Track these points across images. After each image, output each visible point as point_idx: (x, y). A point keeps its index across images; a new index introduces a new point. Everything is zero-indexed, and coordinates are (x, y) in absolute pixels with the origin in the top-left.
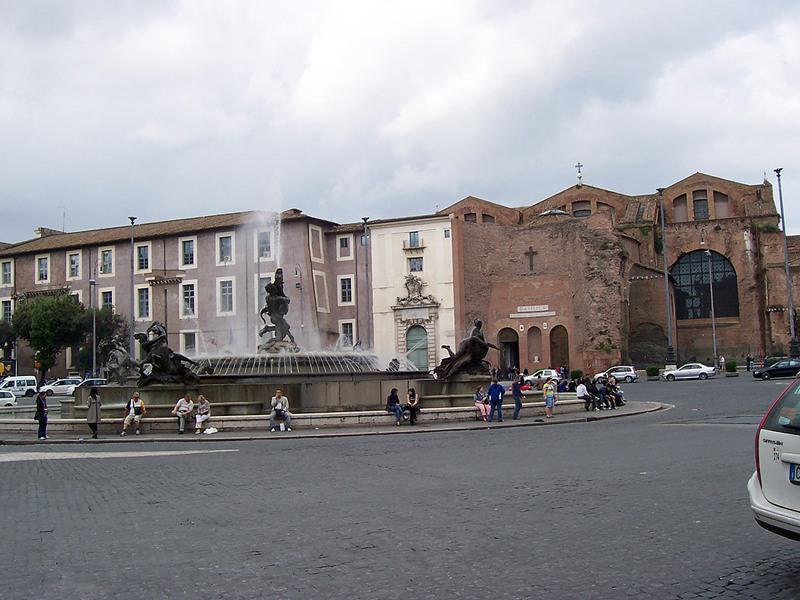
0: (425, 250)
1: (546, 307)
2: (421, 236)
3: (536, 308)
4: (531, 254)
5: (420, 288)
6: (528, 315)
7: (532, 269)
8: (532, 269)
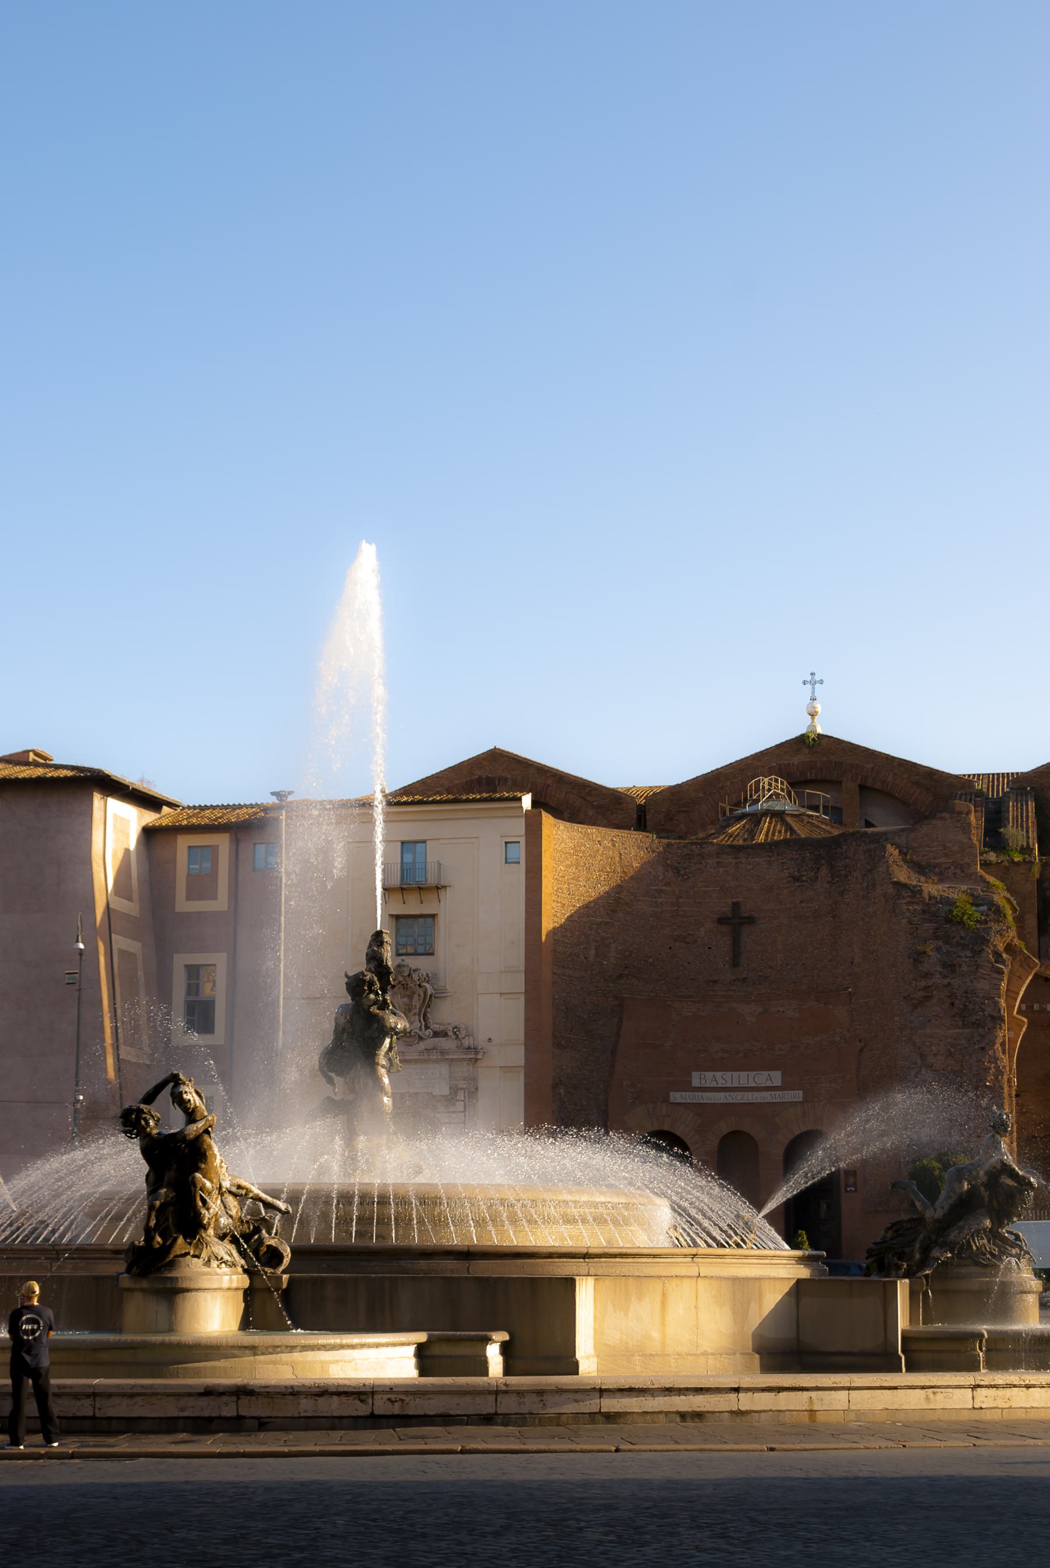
0: (447, 896)
1: (776, 1078)
2: (433, 854)
3: (743, 1078)
4: (736, 921)
5: (428, 1001)
6: (721, 1098)
7: (735, 963)
8: (735, 963)
